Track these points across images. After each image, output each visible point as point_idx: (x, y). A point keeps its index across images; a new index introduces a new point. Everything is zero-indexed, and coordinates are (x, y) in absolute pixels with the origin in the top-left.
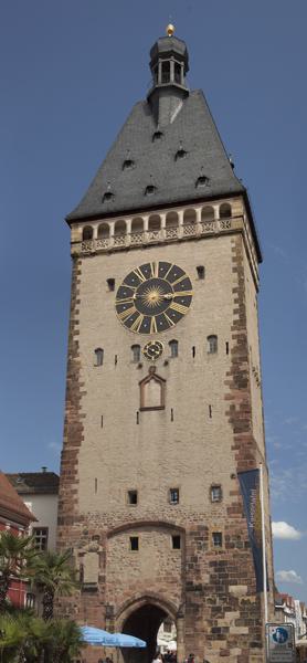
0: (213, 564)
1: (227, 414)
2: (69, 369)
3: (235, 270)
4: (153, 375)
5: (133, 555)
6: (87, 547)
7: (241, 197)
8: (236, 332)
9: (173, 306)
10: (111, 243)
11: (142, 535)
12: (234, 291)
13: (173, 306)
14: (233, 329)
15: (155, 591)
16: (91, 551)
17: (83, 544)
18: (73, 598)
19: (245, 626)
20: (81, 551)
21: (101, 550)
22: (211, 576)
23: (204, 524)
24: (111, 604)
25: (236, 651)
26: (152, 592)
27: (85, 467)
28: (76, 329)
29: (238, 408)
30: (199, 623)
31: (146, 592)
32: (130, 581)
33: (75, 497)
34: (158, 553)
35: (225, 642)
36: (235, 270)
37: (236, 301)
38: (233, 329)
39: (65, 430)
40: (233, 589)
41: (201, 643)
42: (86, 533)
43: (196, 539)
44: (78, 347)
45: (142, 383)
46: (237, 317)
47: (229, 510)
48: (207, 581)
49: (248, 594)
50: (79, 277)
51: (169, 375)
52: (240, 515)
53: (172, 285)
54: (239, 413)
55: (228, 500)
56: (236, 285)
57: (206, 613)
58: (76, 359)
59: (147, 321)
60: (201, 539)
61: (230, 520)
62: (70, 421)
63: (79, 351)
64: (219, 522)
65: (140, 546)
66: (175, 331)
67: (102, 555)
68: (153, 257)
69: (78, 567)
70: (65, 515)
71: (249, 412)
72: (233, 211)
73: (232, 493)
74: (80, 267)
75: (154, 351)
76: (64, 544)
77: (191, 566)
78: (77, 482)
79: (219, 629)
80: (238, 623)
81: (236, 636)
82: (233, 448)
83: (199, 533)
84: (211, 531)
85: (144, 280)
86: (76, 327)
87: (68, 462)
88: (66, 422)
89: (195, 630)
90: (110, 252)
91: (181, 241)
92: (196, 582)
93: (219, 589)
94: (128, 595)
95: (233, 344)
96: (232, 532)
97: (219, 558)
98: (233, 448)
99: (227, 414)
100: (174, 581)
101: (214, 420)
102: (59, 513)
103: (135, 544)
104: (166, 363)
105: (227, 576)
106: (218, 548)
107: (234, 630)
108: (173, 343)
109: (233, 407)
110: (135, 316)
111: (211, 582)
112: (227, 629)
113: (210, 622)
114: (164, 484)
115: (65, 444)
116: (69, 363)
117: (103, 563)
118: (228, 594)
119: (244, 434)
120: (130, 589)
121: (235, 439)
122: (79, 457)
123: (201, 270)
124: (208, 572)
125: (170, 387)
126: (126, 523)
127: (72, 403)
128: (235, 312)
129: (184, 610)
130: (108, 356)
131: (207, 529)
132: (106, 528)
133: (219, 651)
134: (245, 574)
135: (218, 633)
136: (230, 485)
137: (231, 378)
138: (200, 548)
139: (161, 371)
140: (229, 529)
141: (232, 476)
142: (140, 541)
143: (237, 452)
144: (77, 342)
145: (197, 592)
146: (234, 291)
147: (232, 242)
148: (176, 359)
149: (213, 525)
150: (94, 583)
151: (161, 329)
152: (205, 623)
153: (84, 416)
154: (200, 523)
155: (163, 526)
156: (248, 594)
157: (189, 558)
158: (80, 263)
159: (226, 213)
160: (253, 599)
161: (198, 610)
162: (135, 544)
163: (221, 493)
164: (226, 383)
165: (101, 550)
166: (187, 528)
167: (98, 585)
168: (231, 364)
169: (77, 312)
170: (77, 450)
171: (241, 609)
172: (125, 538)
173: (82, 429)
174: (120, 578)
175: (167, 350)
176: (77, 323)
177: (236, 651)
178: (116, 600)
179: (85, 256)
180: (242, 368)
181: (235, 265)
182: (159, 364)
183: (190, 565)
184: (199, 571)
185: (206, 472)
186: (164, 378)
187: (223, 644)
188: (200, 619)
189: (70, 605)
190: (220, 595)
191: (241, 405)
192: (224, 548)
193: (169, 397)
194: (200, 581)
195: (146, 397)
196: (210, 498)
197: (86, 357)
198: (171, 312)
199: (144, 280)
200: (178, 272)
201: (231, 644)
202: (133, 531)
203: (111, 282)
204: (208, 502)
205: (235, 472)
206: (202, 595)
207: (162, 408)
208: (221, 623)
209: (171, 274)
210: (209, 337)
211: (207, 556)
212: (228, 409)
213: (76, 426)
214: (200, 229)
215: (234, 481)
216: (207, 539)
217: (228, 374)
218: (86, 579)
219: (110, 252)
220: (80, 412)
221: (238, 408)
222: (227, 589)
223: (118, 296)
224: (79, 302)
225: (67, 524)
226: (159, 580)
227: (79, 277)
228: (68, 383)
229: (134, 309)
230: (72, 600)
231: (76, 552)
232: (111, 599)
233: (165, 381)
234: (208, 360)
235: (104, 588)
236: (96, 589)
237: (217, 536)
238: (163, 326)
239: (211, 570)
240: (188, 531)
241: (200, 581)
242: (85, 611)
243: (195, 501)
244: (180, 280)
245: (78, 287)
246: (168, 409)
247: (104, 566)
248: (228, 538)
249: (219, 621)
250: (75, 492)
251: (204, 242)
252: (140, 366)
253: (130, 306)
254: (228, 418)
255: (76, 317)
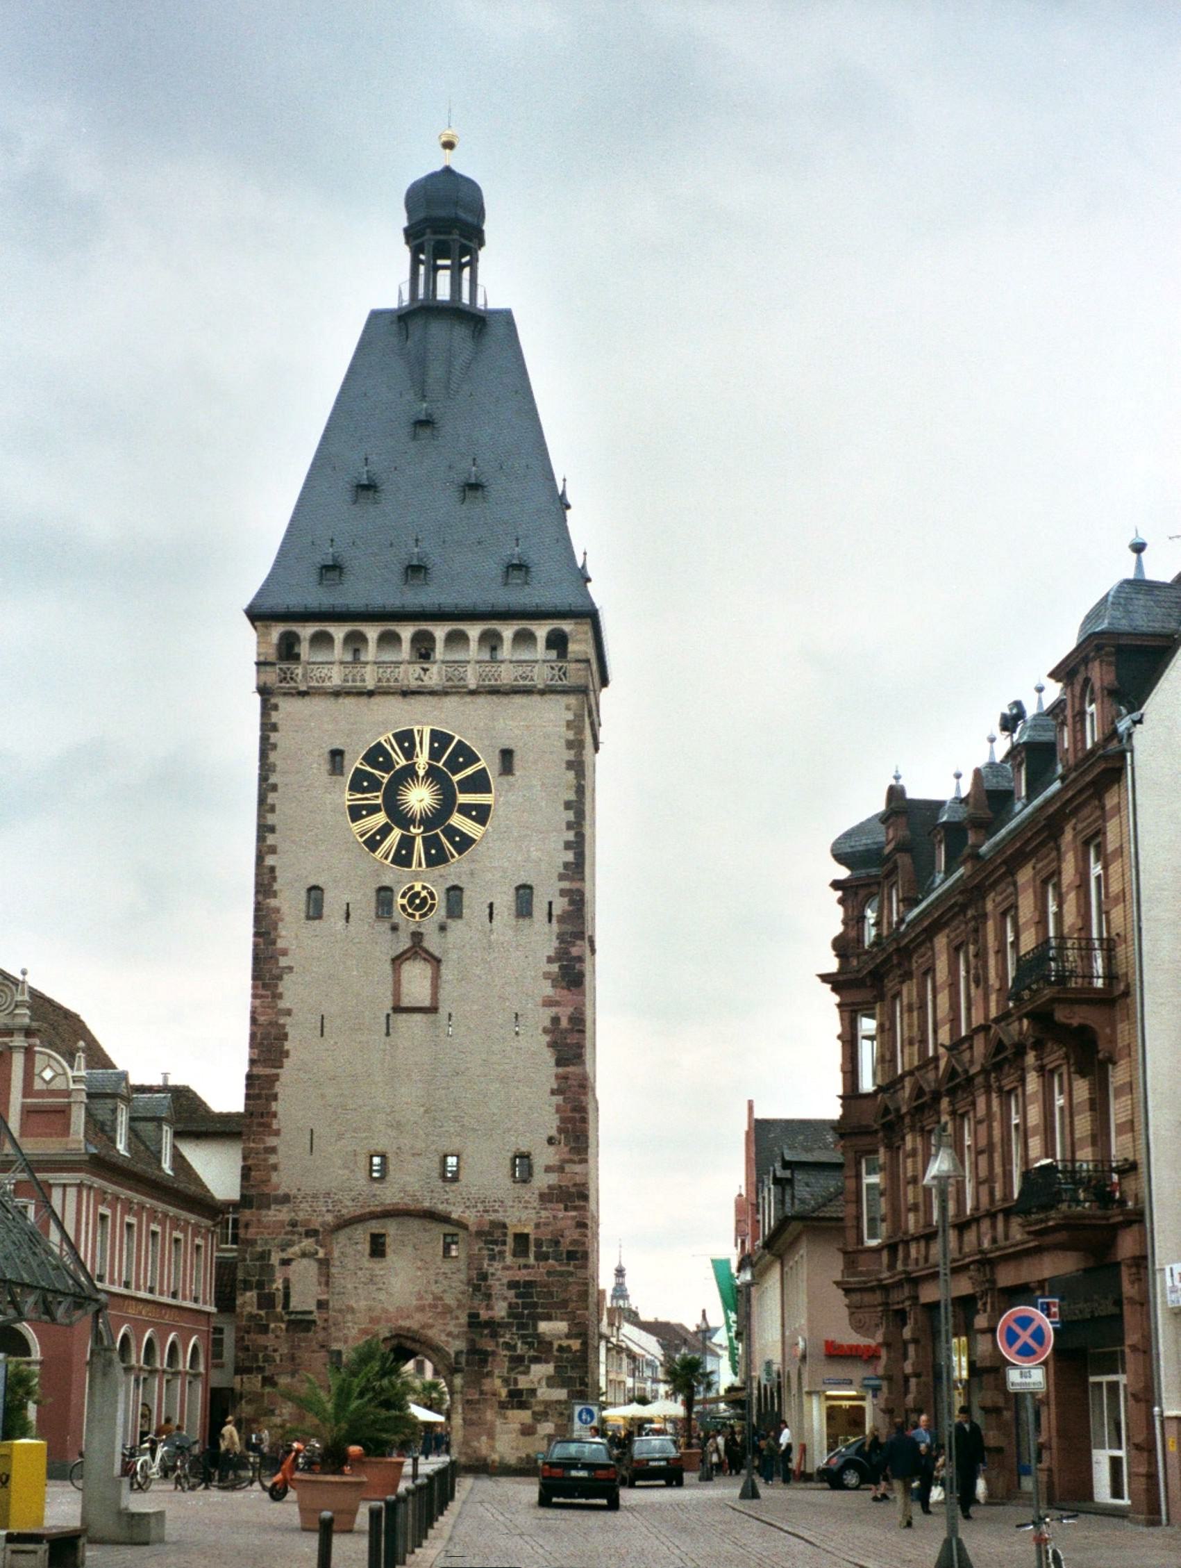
0: (513, 1285)
1: (546, 1031)
2: (258, 920)
3: (570, 765)
4: (417, 949)
5: (377, 1266)
6: (296, 1249)
7: (589, 620)
8: (566, 885)
9: (457, 820)
10: (336, 677)
11: (391, 1229)
12: (568, 805)
13: (457, 820)
14: (562, 877)
15: (415, 1326)
16: (304, 1255)
17: (290, 1244)
18: (271, 1336)
19: (562, 1386)
20: (285, 1256)
21: (321, 1254)
22: (510, 1306)
23: (499, 1217)
24: (335, 1346)
25: (547, 1428)
26: (409, 1329)
27: (290, 1107)
28: (269, 842)
29: (564, 1023)
30: (487, 1381)
31: (401, 1328)
32: (370, 1309)
33: (273, 1159)
34: (419, 1264)
35: (529, 1413)
36: (570, 765)
37: (569, 826)
38: (562, 877)
39: (253, 1036)
40: (543, 1326)
41: (489, 1415)
42: (294, 1224)
43: (486, 1242)
44: (274, 879)
45: (397, 961)
46: (570, 856)
47: (542, 1197)
48: (503, 1313)
49: (568, 1336)
50: (274, 737)
51: (446, 952)
52: (562, 1206)
53: (456, 778)
54: (566, 1030)
55: (542, 1180)
56: (572, 796)
57: (500, 1367)
58: (273, 902)
59: (407, 842)
60: (495, 1242)
61: (544, 1213)
62: (261, 1019)
63: (276, 887)
64: (522, 1216)
65: (388, 1250)
66: (457, 868)
67: (325, 1264)
68: (424, 720)
69: (279, 1284)
70: (253, 1192)
71: (583, 1032)
72: (572, 647)
73: (548, 1169)
74: (275, 717)
75: (419, 903)
76: (252, 1243)
77: (477, 1288)
78: (277, 1133)
79: (519, 1393)
80: (551, 1382)
81: (548, 1404)
82: (553, 1092)
83: (491, 1234)
84: (511, 1231)
85: (401, 762)
86: (271, 839)
87: (258, 1097)
88: (254, 1021)
89: (482, 1393)
90: (337, 694)
91: (472, 693)
92: (484, 1315)
93: (522, 1326)
94: (364, 1332)
95: (560, 905)
96: (546, 1234)
97: (523, 1275)
98: (553, 1092)
99: (546, 1031)
100: (448, 1310)
101: (523, 1042)
102: (242, 1187)
103: (378, 1248)
104: (443, 928)
105: (535, 1305)
106: (522, 1261)
107: (545, 1393)
108: (454, 893)
109: (556, 1020)
110: (385, 831)
111: (510, 1315)
112: (533, 1392)
113: (506, 1381)
114: (433, 1147)
115: (252, 1062)
116: (258, 907)
117: (326, 1277)
118: (538, 1336)
119: (571, 1069)
120: (373, 1320)
121: (557, 1077)
122: (278, 1088)
123: (507, 756)
124: (505, 1299)
125: (445, 970)
126: (368, 1210)
127: (265, 986)
128: (568, 846)
129: (463, 1359)
130: (333, 902)
131: (504, 1226)
132: (329, 1218)
133: (517, 1426)
134: (564, 1304)
135: (518, 1399)
136: (544, 1156)
137: (555, 968)
138: (492, 1258)
139: (432, 942)
140: (542, 1229)
141: (551, 1141)
142: (388, 1240)
143: (558, 1099)
144: (272, 869)
145: (486, 1332)
146: (568, 805)
147: (568, 708)
148: (460, 922)
149: (515, 1221)
150: (311, 1312)
151: (432, 861)
152: (498, 1382)
153: (288, 1013)
154: (493, 1216)
155: (431, 1216)
156: (568, 1336)
157: (474, 1273)
158: (276, 707)
159: (558, 642)
160: (576, 1344)
161: (486, 1361)
162: (378, 1248)
163: (530, 1167)
164: (547, 975)
165: (321, 1254)
166: (470, 1217)
167: (315, 1316)
168: (555, 943)
169: (272, 809)
170: (277, 1075)
171: (558, 1360)
172: (361, 1235)
173: (285, 1037)
174: (353, 1303)
175: (440, 912)
176: (272, 829)
177: (547, 1428)
178: (346, 1342)
179: (285, 694)
180: (575, 951)
181: (570, 755)
182: (429, 926)
183: (479, 1284)
184: (489, 1296)
185: (509, 1130)
186: (437, 954)
187: (525, 1416)
188: (489, 1374)
189: (266, 1348)
190: (523, 1337)
191: (571, 1019)
192: (532, 1260)
193: (443, 994)
194: (490, 1313)
195: (405, 989)
196: (513, 1175)
197: (290, 902)
198: (452, 832)
199: (401, 762)
200: (465, 755)
201: (539, 1417)
202: (378, 1225)
203: (337, 756)
204: (508, 1182)
205: (553, 1132)
206: (494, 1335)
207: (432, 1010)
208: (523, 1383)
209: (452, 755)
210: (518, 888)
211: (502, 1272)
212: (547, 1023)
213: (273, 1031)
214: (507, 675)
215: (552, 1149)
216: (504, 1243)
217: (550, 960)
218: (295, 1304)
219: (337, 694)
220: (283, 1004)
221: (564, 1023)
222: (535, 1327)
223: (355, 786)
224: (274, 788)
225: (259, 1208)
226: (421, 1309)
227: (274, 737)
228: (256, 945)
229: (381, 818)
230: (268, 1340)
231: (275, 1259)
232: (337, 1340)
233: (438, 961)
234: (517, 930)
235: (326, 1320)
236: (314, 1322)
237: (522, 1239)
238: (437, 858)
239: (512, 1292)
240: (473, 1228)
241: (490, 1313)
242: (293, 1358)
243: (485, 1185)
244: (469, 771)
245: (273, 757)
246: (443, 1011)
247: (327, 1284)
248: (539, 1243)
249: (521, 1378)
250: (273, 1150)
251: (519, 700)
252: (395, 928)
253: (373, 810)
254: (547, 1038)
255: (271, 819)
